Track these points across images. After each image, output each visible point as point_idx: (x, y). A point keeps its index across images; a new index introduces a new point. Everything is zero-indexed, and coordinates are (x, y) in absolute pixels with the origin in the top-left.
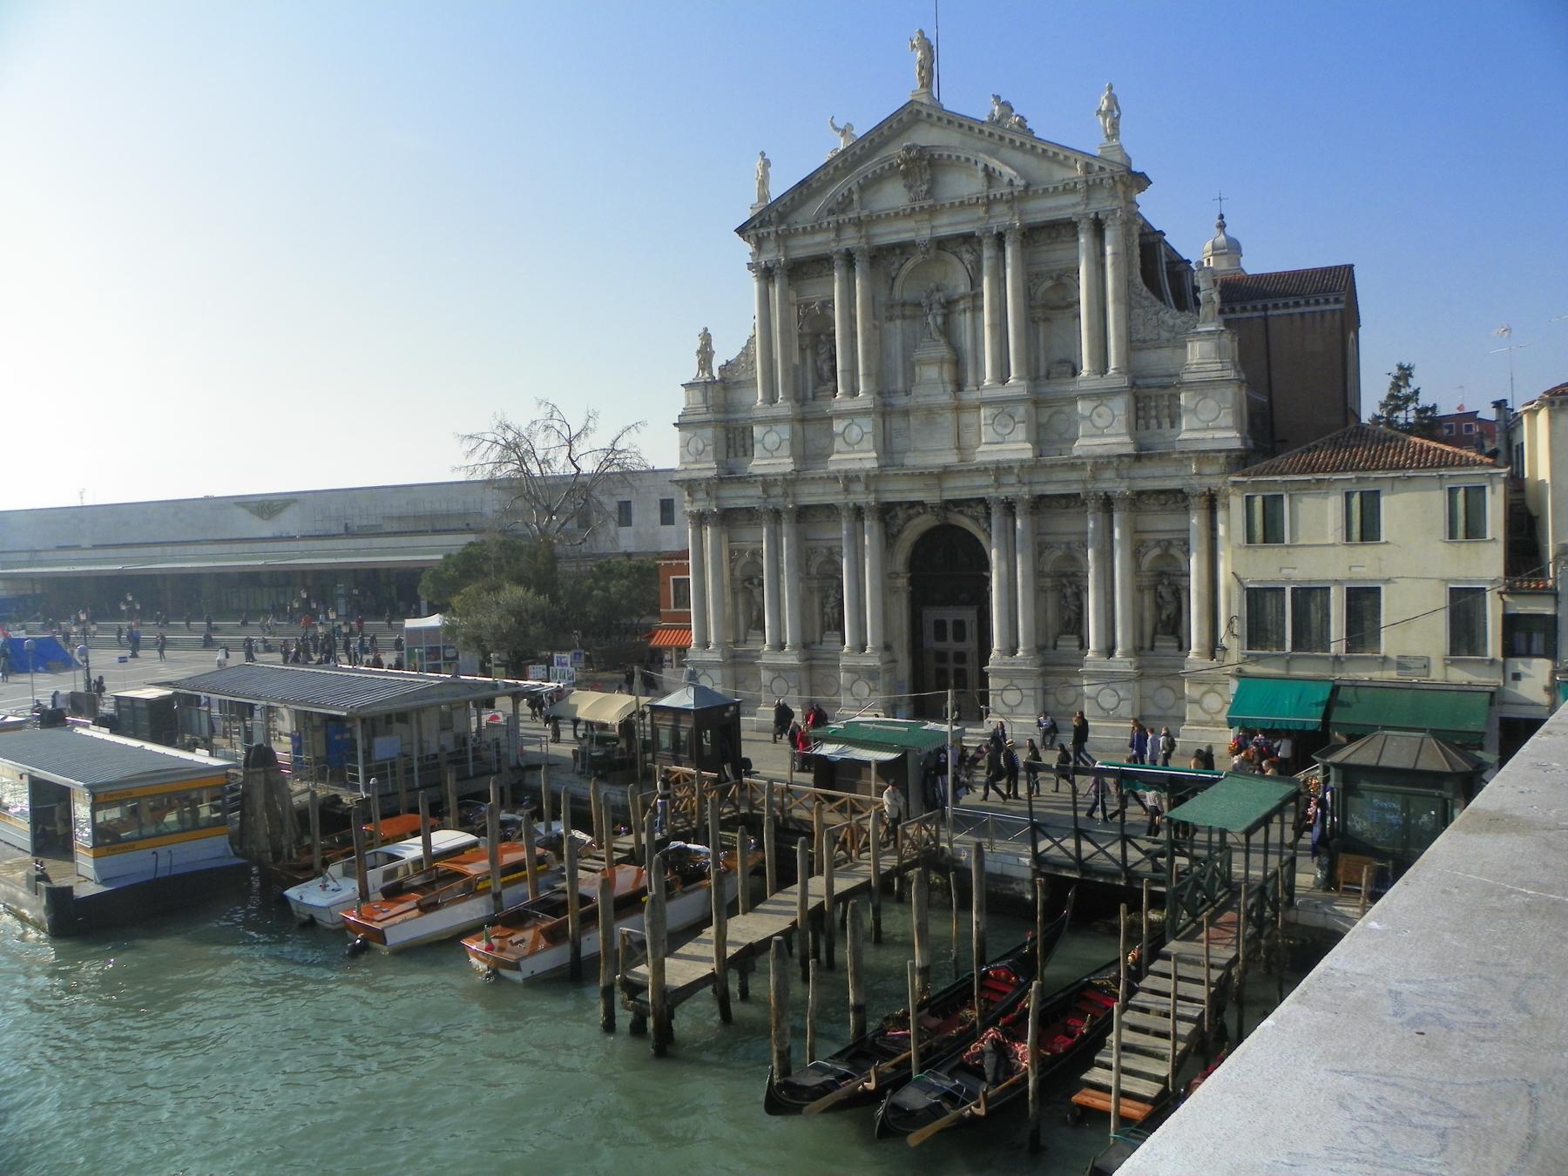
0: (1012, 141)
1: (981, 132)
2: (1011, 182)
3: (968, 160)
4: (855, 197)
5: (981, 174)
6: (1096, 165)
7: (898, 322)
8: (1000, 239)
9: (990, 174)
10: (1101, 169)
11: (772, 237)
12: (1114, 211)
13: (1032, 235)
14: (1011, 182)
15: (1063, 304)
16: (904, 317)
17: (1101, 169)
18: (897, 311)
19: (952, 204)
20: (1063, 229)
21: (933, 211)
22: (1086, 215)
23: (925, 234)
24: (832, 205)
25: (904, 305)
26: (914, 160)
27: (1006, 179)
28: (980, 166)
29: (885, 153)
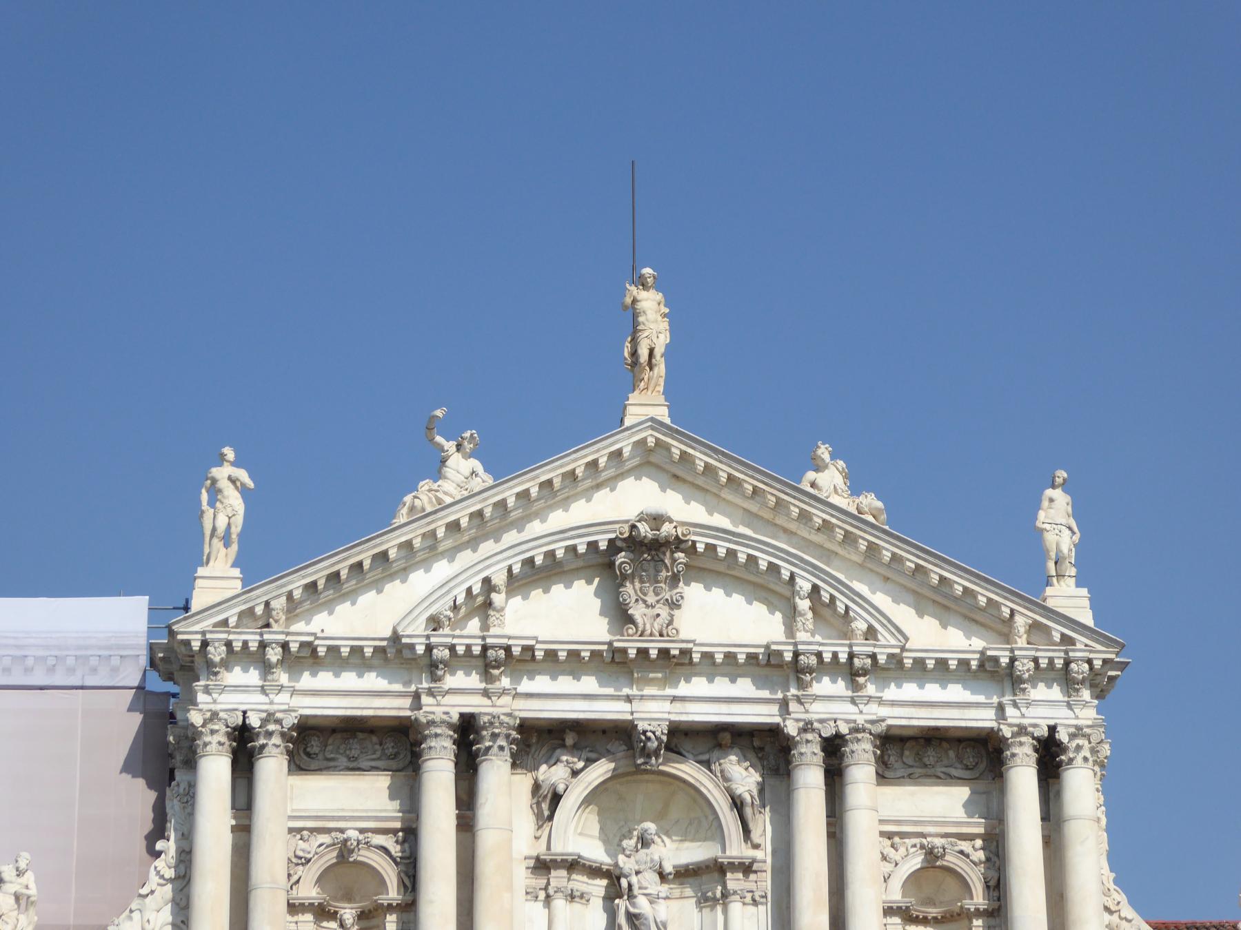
0: (871, 546)
1: (804, 517)
2: (871, 633)
3: (773, 569)
4: (498, 599)
5: (804, 604)
6: (1057, 630)
7: (559, 903)
8: (834, 750)
9: (822, 607)
10: (1066, 640)
11: (274, 655)
12: (1078, 732)
13: (912, 752)
14: (871, 633)
15: (933, 912)
16: (572, 897)
17: (1066, 640)
18: (558, 877)
19: (730, 657)
20: (979, 756)
21: (676, 663)
22: (1022, 730)
23: (653, 709)
24: (442, 607)
25: (573, 865)
26: (657, 547)
27: (860, 626)
28: (804, 585)
29: (558, 519)
